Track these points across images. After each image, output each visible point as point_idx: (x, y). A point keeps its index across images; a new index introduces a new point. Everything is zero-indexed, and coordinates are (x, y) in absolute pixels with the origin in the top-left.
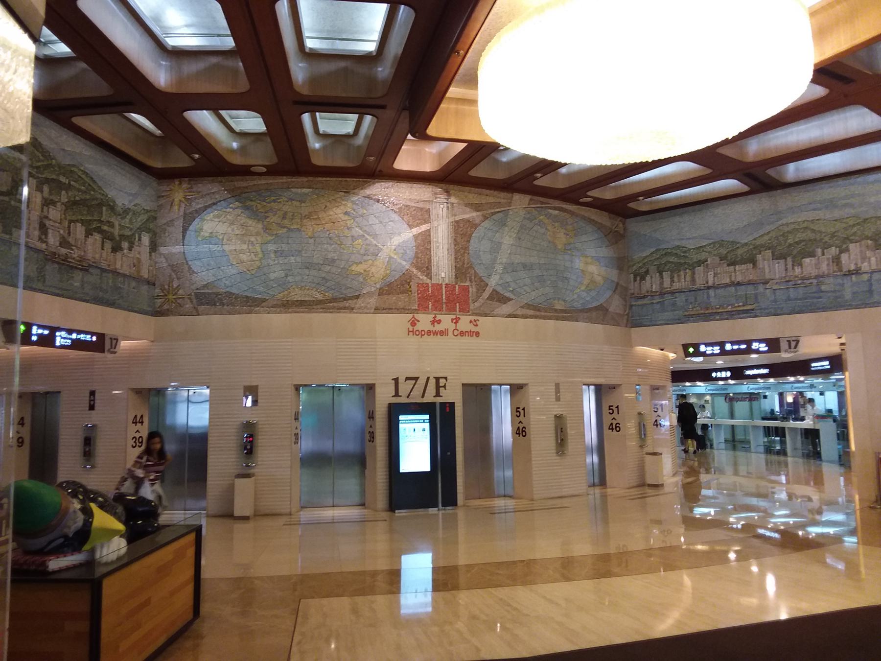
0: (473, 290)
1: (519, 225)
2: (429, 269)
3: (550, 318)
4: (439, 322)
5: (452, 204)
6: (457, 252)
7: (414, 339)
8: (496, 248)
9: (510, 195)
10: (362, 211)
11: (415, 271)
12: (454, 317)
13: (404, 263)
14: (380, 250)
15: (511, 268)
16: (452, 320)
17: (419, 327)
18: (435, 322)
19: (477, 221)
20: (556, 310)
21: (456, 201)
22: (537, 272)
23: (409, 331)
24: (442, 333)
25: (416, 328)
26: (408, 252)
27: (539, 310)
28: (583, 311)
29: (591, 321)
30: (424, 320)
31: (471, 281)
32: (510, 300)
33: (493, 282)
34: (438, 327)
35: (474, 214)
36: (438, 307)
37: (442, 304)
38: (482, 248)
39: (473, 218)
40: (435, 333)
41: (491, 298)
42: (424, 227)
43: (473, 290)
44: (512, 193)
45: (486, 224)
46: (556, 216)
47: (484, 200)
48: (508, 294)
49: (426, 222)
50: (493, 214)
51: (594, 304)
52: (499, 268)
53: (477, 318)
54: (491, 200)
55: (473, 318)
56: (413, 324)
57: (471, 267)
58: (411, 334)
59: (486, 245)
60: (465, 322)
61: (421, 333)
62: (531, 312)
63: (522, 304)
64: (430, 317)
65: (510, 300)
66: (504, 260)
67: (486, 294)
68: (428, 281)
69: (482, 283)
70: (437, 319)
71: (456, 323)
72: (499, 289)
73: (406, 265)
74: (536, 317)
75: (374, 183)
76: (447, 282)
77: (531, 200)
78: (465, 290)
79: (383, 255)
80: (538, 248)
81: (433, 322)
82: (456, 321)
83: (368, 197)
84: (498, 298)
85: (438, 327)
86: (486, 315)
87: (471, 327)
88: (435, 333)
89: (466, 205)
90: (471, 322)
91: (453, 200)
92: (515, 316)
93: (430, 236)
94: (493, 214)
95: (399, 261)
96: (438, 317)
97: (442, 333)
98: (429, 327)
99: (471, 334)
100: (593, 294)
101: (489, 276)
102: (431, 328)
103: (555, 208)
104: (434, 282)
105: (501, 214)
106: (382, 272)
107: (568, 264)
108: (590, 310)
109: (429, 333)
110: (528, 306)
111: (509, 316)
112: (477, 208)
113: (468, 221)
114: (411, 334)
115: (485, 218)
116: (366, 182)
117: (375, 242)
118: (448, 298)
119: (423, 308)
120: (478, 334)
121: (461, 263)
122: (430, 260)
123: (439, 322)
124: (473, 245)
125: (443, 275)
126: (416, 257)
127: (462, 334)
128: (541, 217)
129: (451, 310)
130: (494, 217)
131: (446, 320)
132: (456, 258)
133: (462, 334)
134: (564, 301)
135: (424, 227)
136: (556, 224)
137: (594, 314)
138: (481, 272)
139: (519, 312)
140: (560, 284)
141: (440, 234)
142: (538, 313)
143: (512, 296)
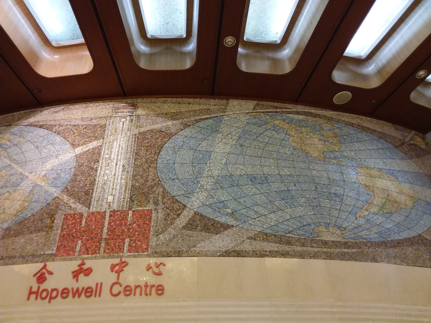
0: (158, 216)
1: (240, 130)
2: (88, 193)
3: (315, 256)
4: (88, 272)
5: (138, 116)
6: (136, 166)
7: (37, 306)
8: (203, 158)
9: (224, 101)
10: (17, 140)
11: (65, 198)
12: (117, 261)
13: (52, 190)
14: (23, 177)
15: (227, 181)
16: (113, 267)
17: (50, 283)
18: (82, 271)
19: (173, 131)
20: (325, 243)
21: (144, 113)
22: (276, 186)
23: (31, 293)
24: (89, 292)
25: (43, 286)
26: (62, 175)
27: (289, 243)
28: (384, 244)
29: (404, 260)
30: (61, 272)
31: (156, 203)
32: (226, 227)
33: (196, 203)
34: (84, 282)
35: (170, 123)
36: (91, 249)
37: (100, 241)
38: (178, 160)
39: (168, 128)
40: (77, 293)
41: (191, 225)
42: (95, 144)
43: (158, 216)
44: (228, 99)
45: (187, 132)
46: (300, 121)
47: (184, 108)
48: (223, 219)
49: (96, 138)
50: (197, 121)
51: (405, 235)
52: (207, 183)
53: (159, 260)
54: (197, 107)
55: (152, 261)
56: (41, 278)
57: (159, 184)
58: (33, 296)
59: (186, 155)
60: (137, 270)
61: (50, 296)
62: (274, 247)
63: (251, 234)
64: (74, 265)
65: (226, 227)
66: (216, 173)
67: (182, 221)
68: (80, 208)
69: (176, 206)
70: (85, 267)
71: (118, 272)
72: (208, 212)
73: (55, 192)
74: (285, 255)
75: (41, 111)
76: (115, 207)
77: (257, 105)
78: (145, 217)
79: (26, 186)
80: (275, 156)
81: (76, 275)
82: (119, 269)
83: (31, 125)
84: (207, 225)
85: (84, 282)
86: (179, 254)
87: (147, 278)
88: (77, 293)
89: (158, 115)
90: (149, 268)
91: (140, 112)
92: (238, 254)
93: (99, 154)
94: (197, 121)
95: (47, 188)
96: (88, 264)
97: (89, 292)
98: (71, 284)
99: (146, 290)
100: (397, 218)
101: (188, 195)
102: (71, 284)
103: (298, 113)
104: (93, 209)
105: (210, 121)
106: (17, 206)
107: (337, 176)
108: (399, 243)
109: (65, 293)
110: (265, 236)
111: (227, 254)
112: (173, 116)
113: (161, 131)
114: (33, 296)
115: (186, 126)
116: (33, 112)
117: (21, 170)
118: (111, 230)
119: (65, 250)
120: (160, 290)
121: (141, 181)
122: (93, 183)
123: (88, 272)
124: (165, 155)
125: (110, 199)
126: (74, 180)
127: (128, 291)
128: (277, 122)
129: (114, 248)
130: (201, 124)
131: (101, 268)
132: (134, 176)
133: (128, 291)
134: (339, 228)
135: (95, 144)
136: (303, 130)
137: (409, 250)
138: (174, 189)
139: (247, 246)
140: (326, 203)
141: (115, 149)
142: (287, 248)
143: (234, 223)
